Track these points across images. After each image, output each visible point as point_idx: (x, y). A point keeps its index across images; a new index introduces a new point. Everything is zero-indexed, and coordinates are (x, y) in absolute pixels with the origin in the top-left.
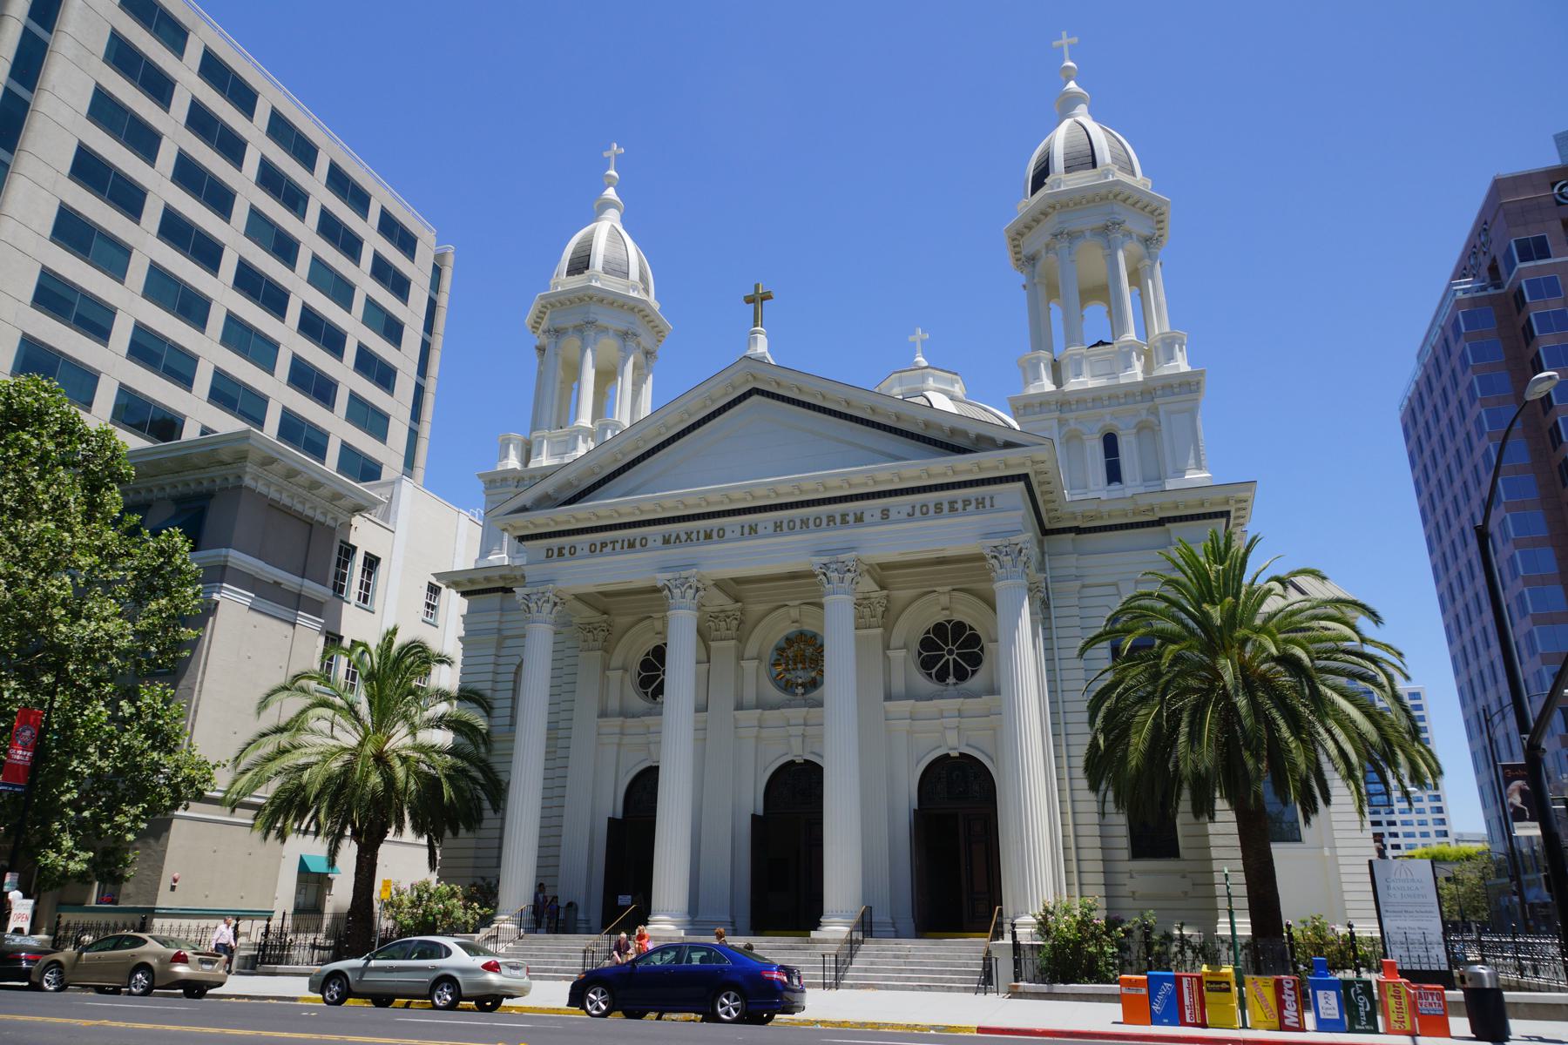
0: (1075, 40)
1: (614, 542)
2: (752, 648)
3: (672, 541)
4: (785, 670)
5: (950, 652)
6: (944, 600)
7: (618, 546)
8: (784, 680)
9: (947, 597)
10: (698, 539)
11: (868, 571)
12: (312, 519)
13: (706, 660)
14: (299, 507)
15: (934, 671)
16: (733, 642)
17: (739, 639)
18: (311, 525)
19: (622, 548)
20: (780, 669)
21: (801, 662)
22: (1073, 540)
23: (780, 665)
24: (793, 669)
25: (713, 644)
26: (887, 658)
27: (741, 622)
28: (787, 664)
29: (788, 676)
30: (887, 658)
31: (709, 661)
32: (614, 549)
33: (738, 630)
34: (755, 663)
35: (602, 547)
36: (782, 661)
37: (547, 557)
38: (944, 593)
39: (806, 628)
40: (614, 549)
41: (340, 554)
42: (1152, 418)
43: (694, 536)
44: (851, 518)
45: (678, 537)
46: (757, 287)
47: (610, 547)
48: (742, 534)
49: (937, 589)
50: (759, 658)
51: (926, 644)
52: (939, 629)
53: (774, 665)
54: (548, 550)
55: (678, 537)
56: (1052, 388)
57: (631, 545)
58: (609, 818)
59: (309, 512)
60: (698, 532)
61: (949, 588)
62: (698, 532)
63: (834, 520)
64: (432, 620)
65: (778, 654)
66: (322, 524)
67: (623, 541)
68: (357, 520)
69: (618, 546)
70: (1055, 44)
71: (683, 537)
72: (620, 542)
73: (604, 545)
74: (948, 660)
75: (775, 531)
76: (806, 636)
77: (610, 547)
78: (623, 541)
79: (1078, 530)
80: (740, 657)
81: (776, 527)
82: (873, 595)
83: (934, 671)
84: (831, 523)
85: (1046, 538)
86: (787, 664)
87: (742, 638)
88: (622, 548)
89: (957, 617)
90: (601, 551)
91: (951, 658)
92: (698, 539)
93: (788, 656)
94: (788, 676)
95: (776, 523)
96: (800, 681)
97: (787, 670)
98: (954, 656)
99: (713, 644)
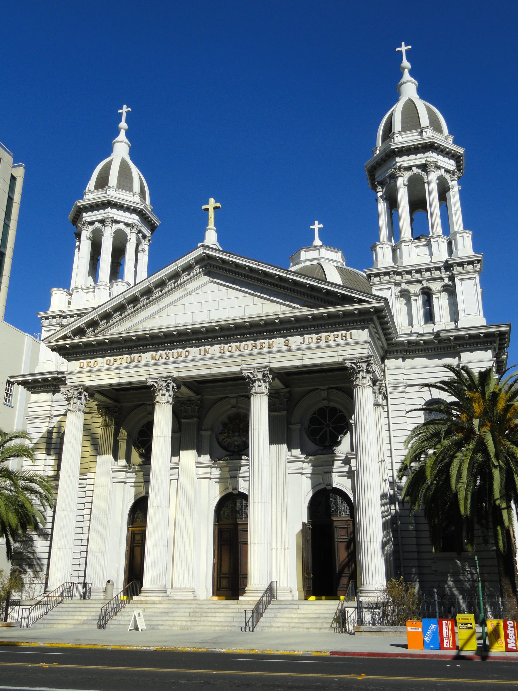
4: (227, 437)
5: (328, 426)
6: (324, 394)
8: (227, 442)
9: (326, 392)
15: (318, 437)
16: (195, 420)
17: (198, 417)
20: (224, 436)
23: (224, 433)
24: (232, 436)
25: (183, 421)
26: (289, 429)
28: (229, 433)
29: (229, 440)
30: (289, 429)
31: (180, 431)
34: (209, 433)
38: (324, 390)
49: (319, 387)
50: (211, 429)
51: (313, 421)
52: (321, 412)
53: (221, 433)
61: (327, 387)
64: (9, 404)
65: (223, 427)
74: (326, 431)
80: (200, 428)
82: (281, 391)
83: (318, 437)
86: (229, 433)
89: (333, 404)
91: (328, 430)
94: (229, 440)
96: (236, 443)
97: (228, 437)
98: (330, 428)
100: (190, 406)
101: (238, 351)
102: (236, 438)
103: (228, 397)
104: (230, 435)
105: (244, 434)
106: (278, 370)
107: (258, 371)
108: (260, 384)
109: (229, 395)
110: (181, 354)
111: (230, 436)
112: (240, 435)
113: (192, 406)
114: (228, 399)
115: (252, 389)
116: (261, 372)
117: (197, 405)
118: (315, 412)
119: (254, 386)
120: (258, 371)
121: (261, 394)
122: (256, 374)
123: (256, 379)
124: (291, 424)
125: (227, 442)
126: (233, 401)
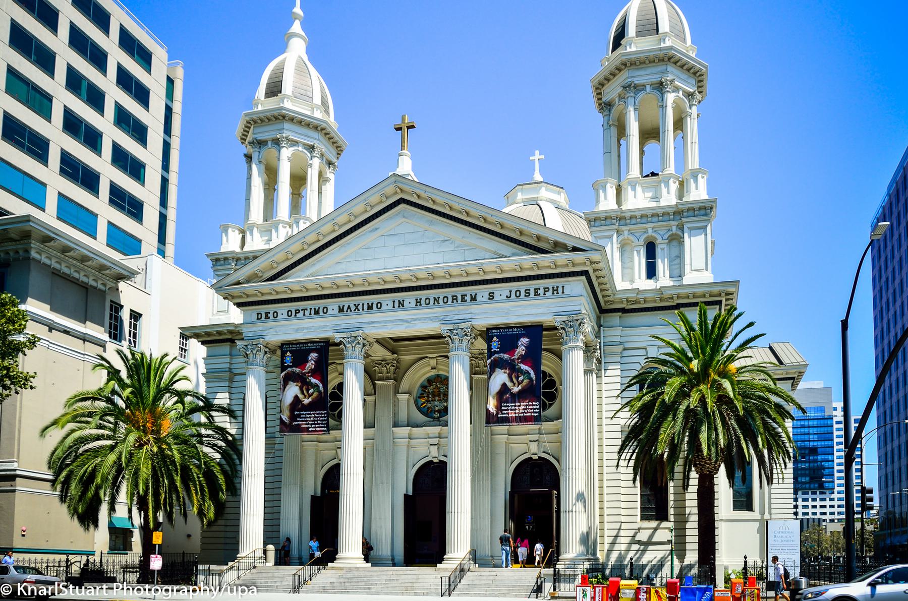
0: (543, 157)
1: (304, 310)
2: (405, 384)
3: (345, 310)
4: (426, 401)
7: (307, 313)
10: (363, 310)
11: (480, 335)
12: (87, 284)
13: (373, 393)
14: (76, 275)
16: (391, 382)
17: (395, 379)
18: (87, 288)
19: (310, 314)
20: (423, 400)
21: (437, 396)
22: (620, 317)
23: (424, 397)
24: (432, 401)
25: (378, 383)
27: (397, 368)
28: (428, 397)
29: (429, 405)
31: (375, 394)
32: (304, 315)
33: (394, 373)
35: (296, 313)
36: (425, 395)
37: (258, 319)
39: (441, 373)
40: (304, 315)
41: (111, 310)
42: (679, 233)
43: (360, 307)
44: (468, 298)
45: (349, 307)
46: (403, 119)
47: (302, 313)
48: (394, 307)
50: (409, 392)
53: (419, 397)
54: (258, 314)
55: (349, 307)
56: (616, 207)
57: (317, 312)
58: (311, 496)
59: (85, 279)
60: (363, 304)
62: (363, 304)
63: (456, 299)
66: (95, 288)
67: (311, 309)
68: (122, 285)
69: (307, 313)
70: (531, 158)
71: (353, 308)
72: (309, 310)
73: (297, 311)
75: (416, 305)
76: (441, 378)
77: (302, 313)
78: (311, 309)
79: (624, 311)
80: (397, 391)
81: (417, 302)
84: (455, 301)
85: (603, 315)
86: (428, 397)
87: (398, 379)
88: (310, 314)
90: (295, 316)
92: (363, 310)
93: (429, 392)
94: (429, 405)
95: (417, 300)
96: (437, 408)
97: (428, 401)
99: (378, 383)
100: (386, 367)
102: (436, 403)
103: (427, 357)
104: (430, 399)
109: (427, 355)
110: (453, 299)
111: (429, 401)
112: (441, 400)
113: (388, 367)
114: (427, 359)
117: (393, 366)
125: (426, 407)
126: (433, 362)
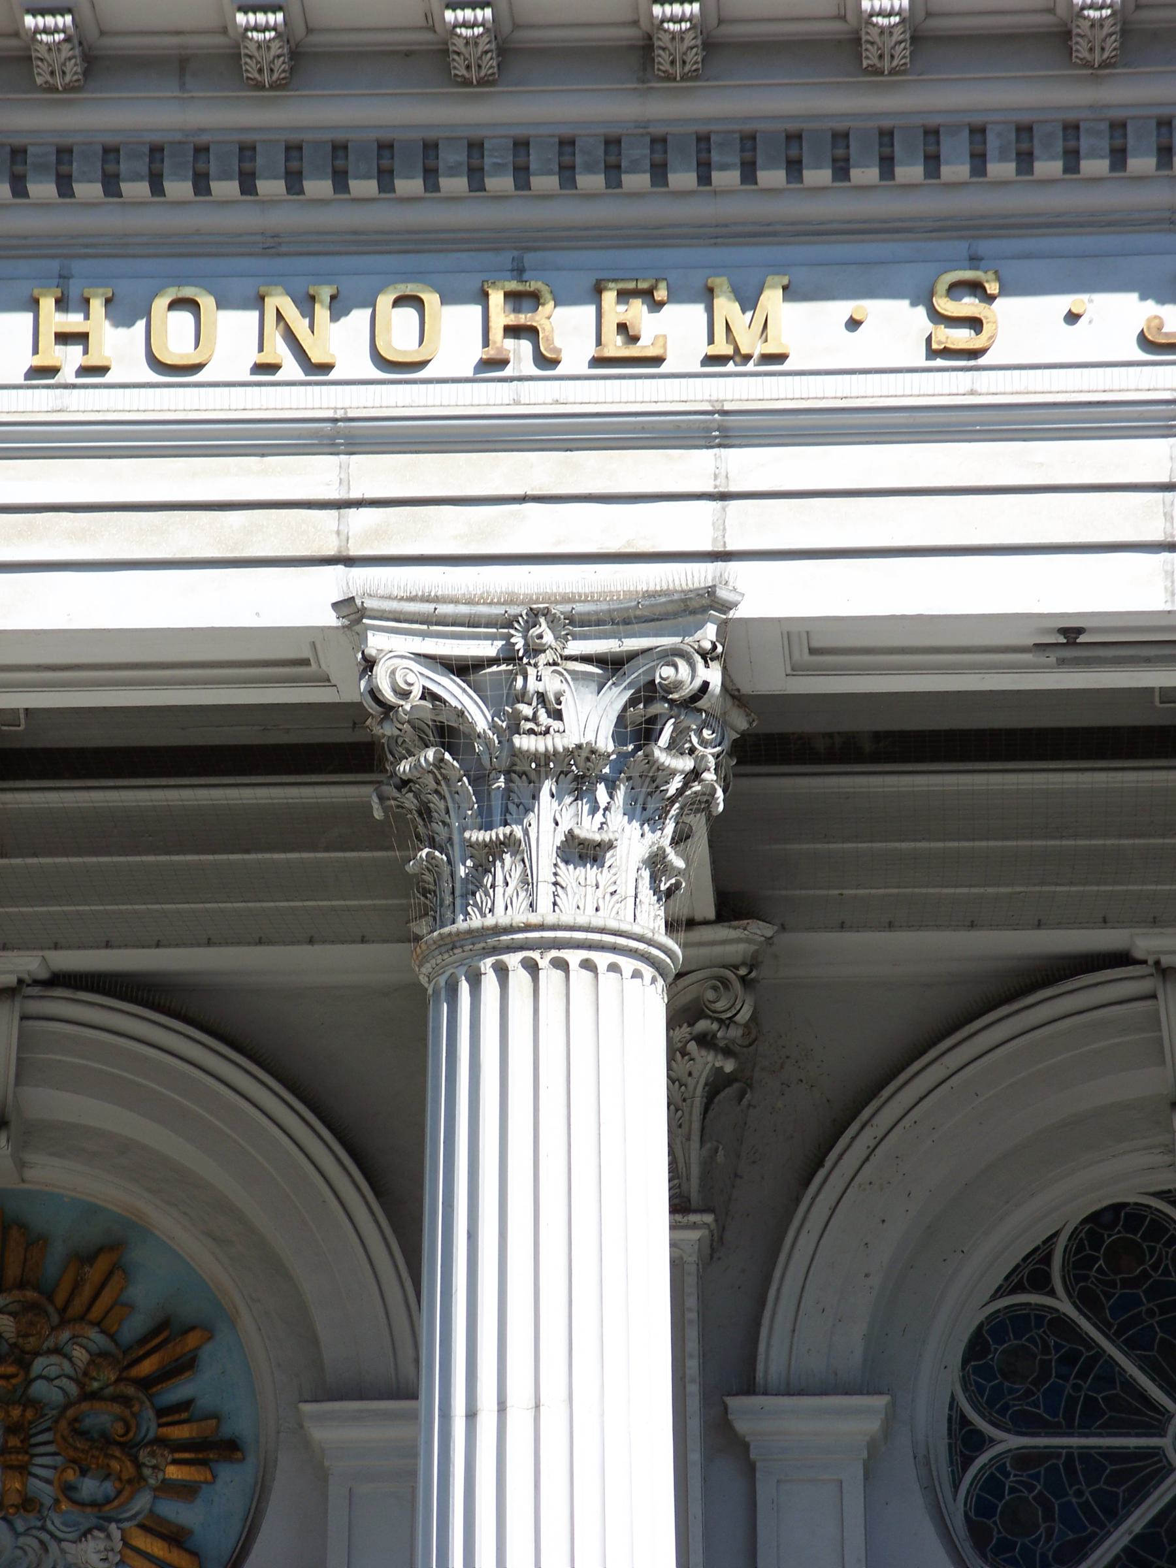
76: (37, 1242)
101: (291, 369)
105: (90, 1487)
106: (797, 670)
107: (576, 647)
108: (589, 829)
115: (473, 885)
116: (613, 665)
118: (1040, 1256)
119: (510, 845)
120: (576, 647)
121: (602, 959)
122: (551, 684)
123: (543, 760)
124: (749, 1388)
